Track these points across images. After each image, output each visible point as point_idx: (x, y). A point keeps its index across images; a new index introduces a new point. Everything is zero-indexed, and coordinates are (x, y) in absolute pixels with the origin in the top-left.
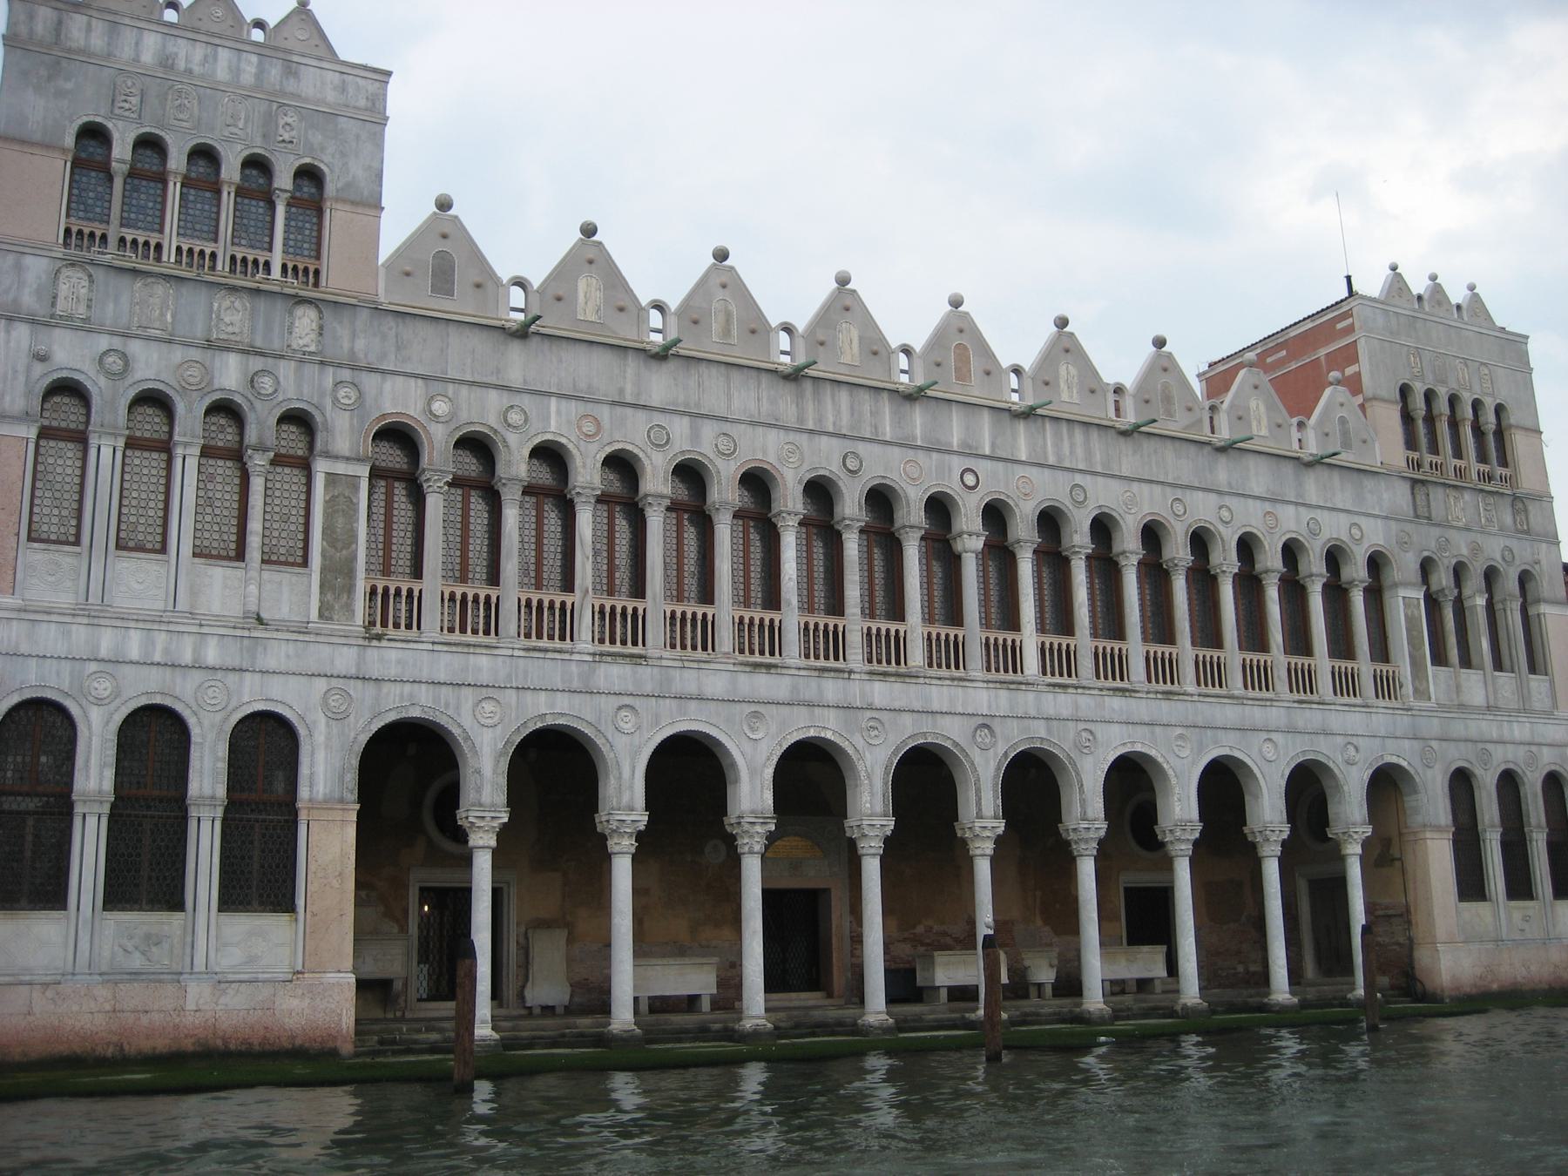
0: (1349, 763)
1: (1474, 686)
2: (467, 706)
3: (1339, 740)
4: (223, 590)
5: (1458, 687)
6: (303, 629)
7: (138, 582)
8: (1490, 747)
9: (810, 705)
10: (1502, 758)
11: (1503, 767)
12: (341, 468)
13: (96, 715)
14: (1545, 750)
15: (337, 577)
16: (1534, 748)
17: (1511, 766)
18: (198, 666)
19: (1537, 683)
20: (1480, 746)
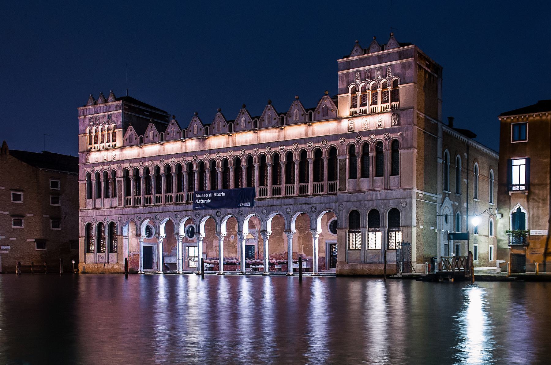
0: (312, 212)
1: (365, 184)
2: (136, 218)
3: (310, 206)
4: (108, 202)
5: (358, 185)
6: (115, 207)
7: (99, 202)
8: (366, 202)
9: (186, 211)
10: (370, 206)
11: (371, 208)
12: (119, 179)
13: (94, 224)
14: (391, 201)
15: (120, 199)
16: (385, 201)
17: (375, 208)
18: (104, 215)
19: (394, 179)
20: (362, 202)
